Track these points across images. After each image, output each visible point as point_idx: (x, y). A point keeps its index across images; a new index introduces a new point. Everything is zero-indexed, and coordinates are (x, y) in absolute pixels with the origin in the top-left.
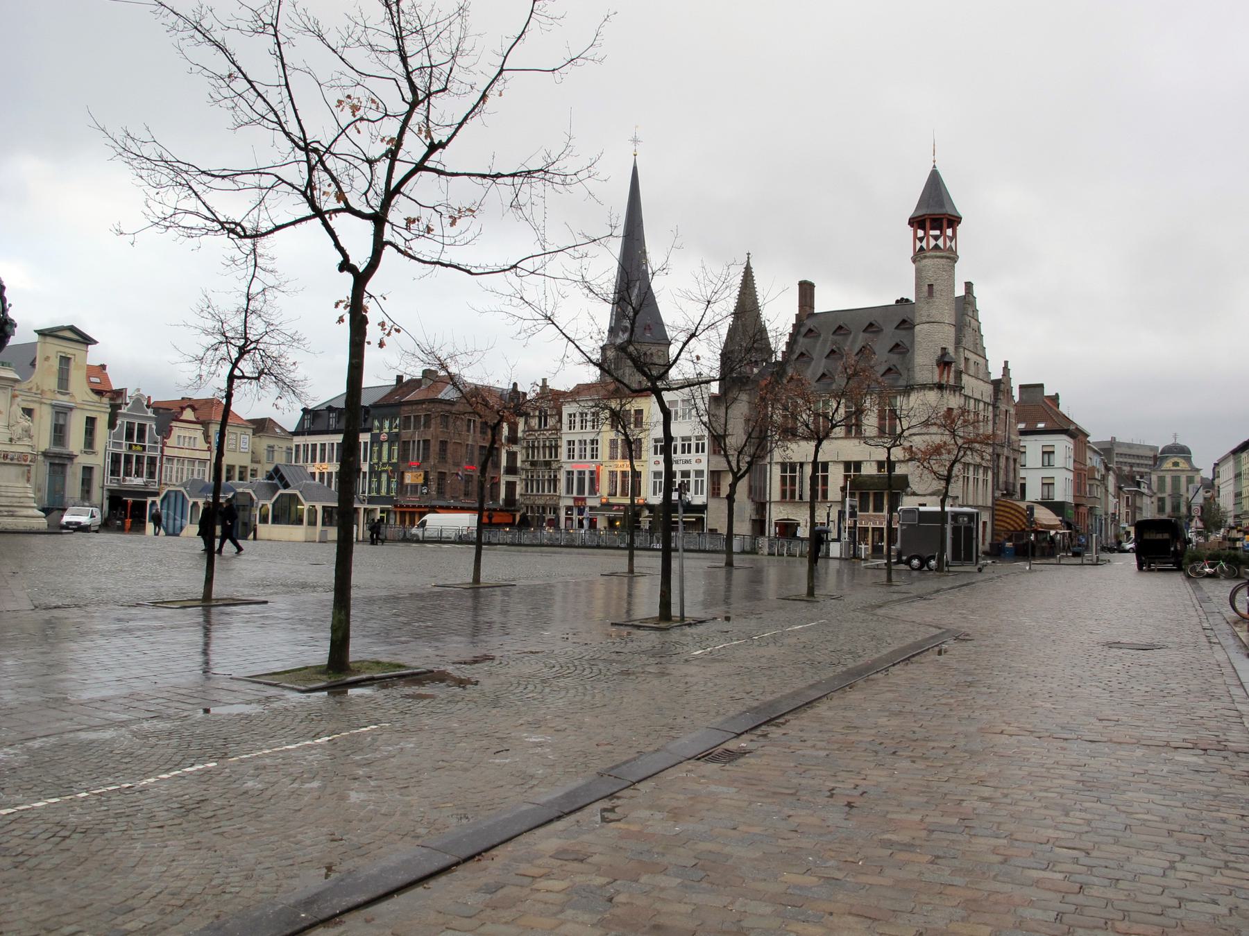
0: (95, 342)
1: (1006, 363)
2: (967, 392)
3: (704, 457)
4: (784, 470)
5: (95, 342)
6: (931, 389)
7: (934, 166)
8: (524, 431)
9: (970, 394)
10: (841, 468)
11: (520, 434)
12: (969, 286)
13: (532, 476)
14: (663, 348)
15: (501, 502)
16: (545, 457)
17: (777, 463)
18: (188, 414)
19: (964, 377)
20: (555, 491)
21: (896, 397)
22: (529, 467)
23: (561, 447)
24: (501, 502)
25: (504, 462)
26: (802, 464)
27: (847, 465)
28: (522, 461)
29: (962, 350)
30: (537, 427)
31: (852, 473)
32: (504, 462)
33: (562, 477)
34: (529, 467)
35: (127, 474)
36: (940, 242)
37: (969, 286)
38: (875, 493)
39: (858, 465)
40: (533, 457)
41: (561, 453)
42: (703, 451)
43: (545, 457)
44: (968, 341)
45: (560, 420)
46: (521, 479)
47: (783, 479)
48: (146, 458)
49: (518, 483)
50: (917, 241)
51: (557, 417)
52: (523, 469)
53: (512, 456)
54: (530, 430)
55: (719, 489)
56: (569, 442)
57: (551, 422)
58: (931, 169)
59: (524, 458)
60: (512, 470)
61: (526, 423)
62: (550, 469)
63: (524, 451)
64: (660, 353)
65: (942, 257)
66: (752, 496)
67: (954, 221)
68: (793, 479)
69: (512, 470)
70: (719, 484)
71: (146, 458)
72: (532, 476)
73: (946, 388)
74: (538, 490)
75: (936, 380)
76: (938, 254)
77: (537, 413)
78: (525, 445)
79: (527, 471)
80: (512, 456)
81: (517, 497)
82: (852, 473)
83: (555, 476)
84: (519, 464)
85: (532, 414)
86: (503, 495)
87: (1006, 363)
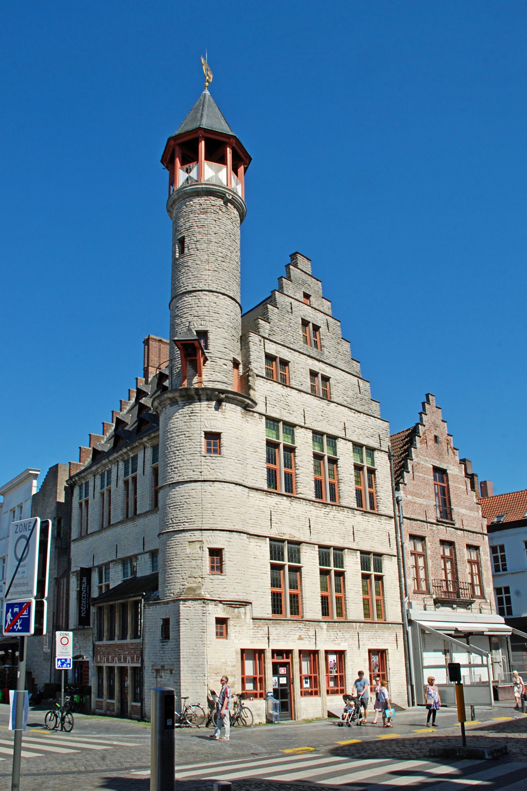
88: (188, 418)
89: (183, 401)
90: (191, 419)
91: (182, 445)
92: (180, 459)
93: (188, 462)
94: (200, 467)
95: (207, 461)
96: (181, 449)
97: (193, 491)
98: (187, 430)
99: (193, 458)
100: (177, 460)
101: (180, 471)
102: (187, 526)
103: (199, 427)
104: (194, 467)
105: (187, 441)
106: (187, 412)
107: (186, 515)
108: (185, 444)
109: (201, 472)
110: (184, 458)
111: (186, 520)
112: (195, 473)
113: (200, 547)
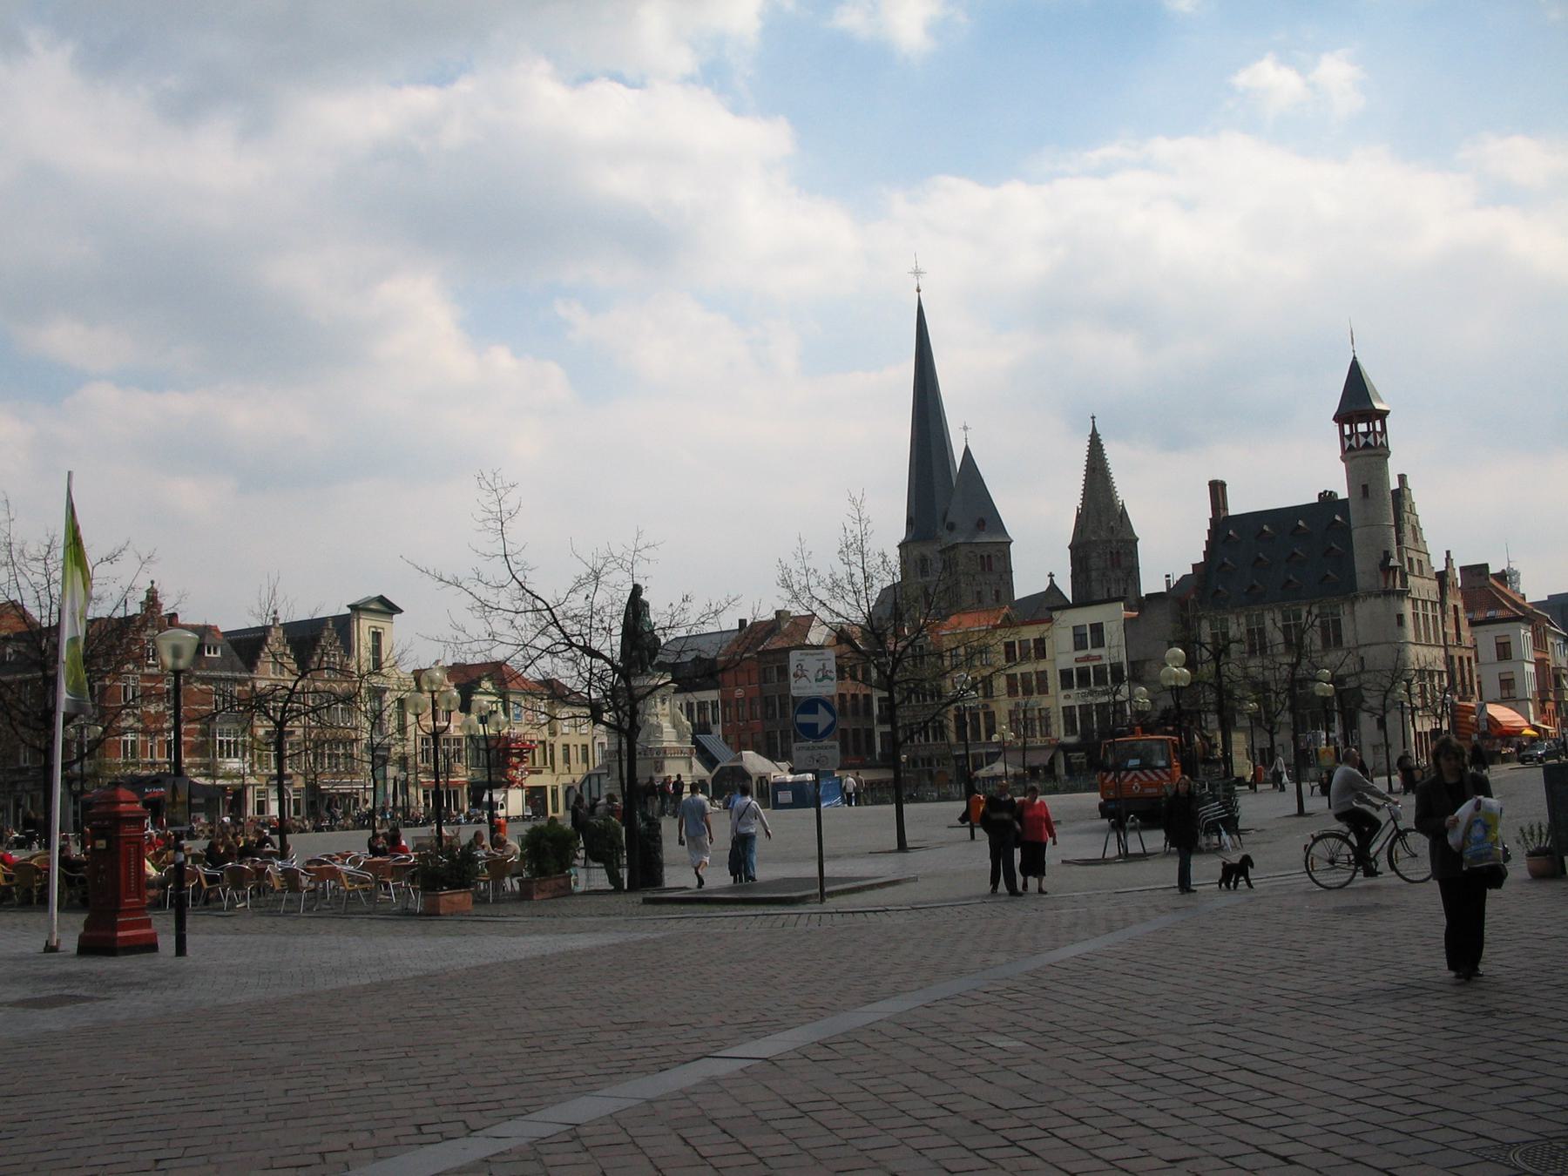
0: (401, 611)
1: (1448, 553)
2: (1415, 594)
5: (401, 611)
6: (1378, 596)
7: (1355, 358)
9: (1417, 597)
12: (1402, 478)
18: (487, 685)
19: (1410, 578)
24: (877, 757)
29: (1404, 550)
35: (856, 732)
36: (1371, 439)
37: (1402, 478)
44: (1408, 540)
48: (1077, 709)
50: (1345, 439)
71: (1077, 709)
87: (1448, 553)
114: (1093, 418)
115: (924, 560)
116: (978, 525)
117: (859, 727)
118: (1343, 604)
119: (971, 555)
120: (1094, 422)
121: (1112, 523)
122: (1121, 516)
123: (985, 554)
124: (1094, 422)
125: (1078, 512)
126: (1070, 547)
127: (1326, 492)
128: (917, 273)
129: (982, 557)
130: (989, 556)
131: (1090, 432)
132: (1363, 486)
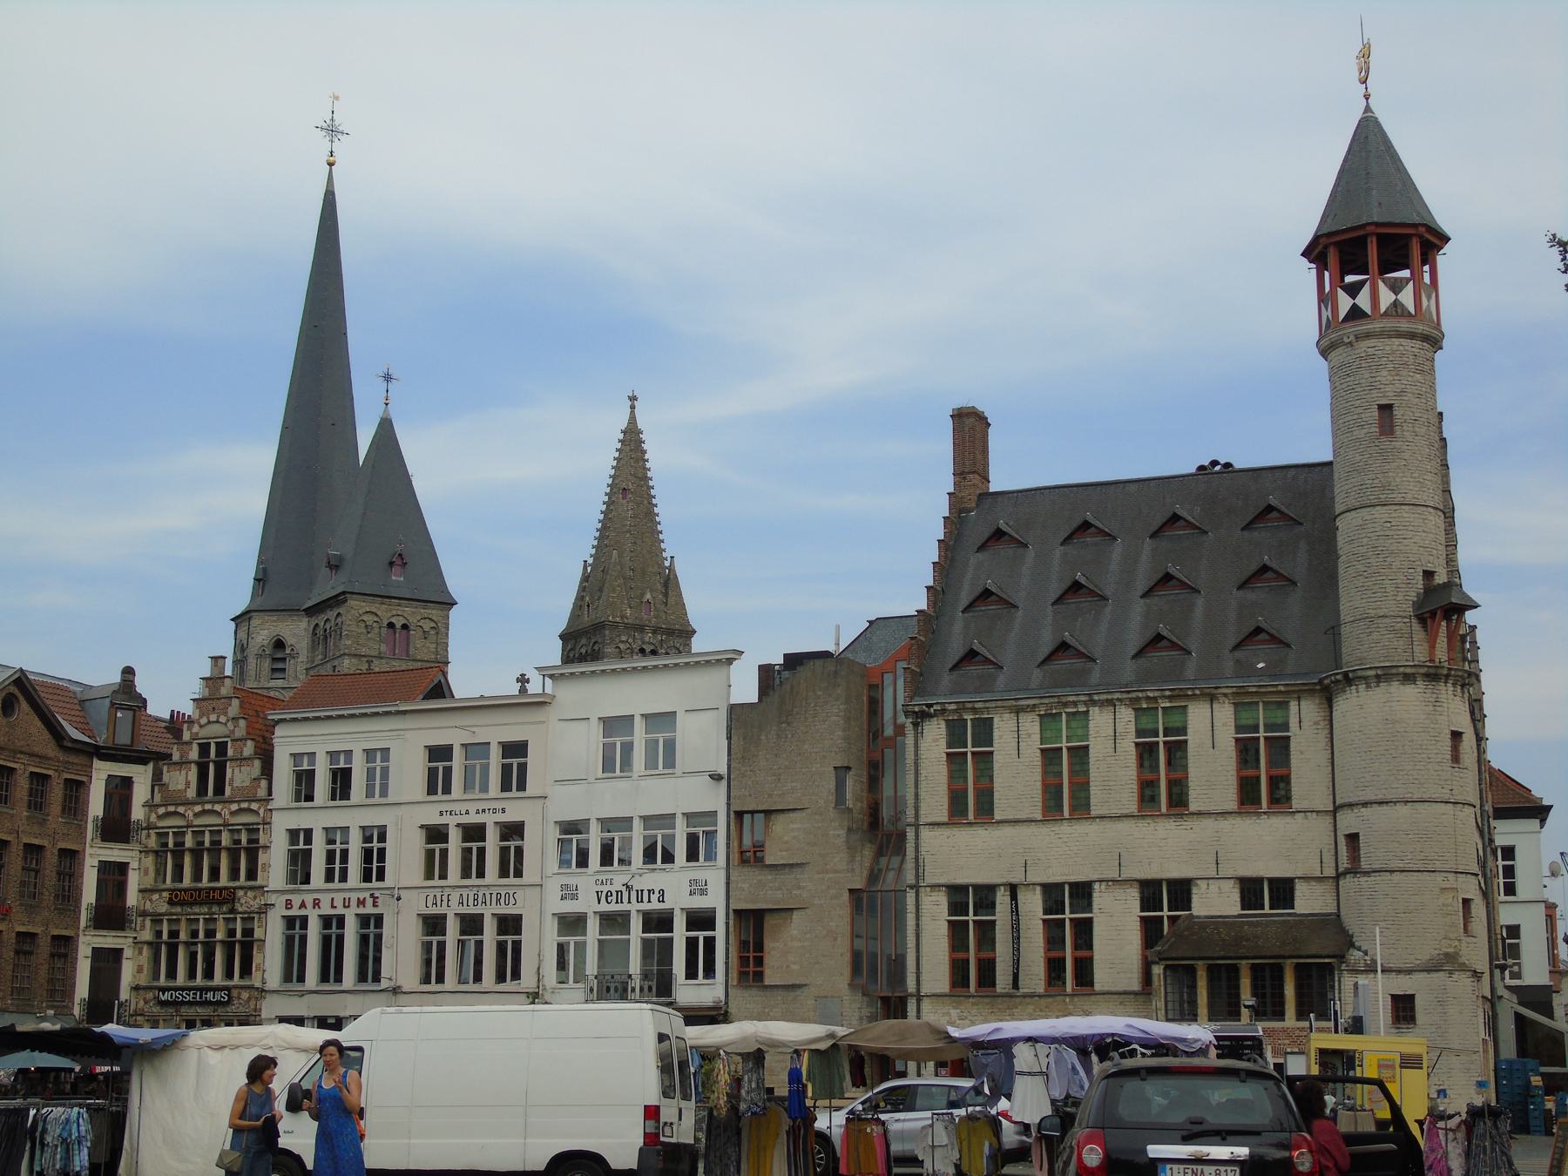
3: (714, 876)
4: (957, 907)
6: (1408, 678)
7: (1368, 109)
8: (150, 805)
10: (1133, 897)
11: (138, 813)
13: (174, 934)
14: (434, 613)
15: (77, 1011)
16: (215, 874)
17: (935, 887)
20: (246, 970)
21: (1284, 705)
22: (164, 908)
23: (266, 847)
24: (77, 1011)
25: (89, 894)
26: (1013, 889)
27: (1150, 892)
28: (141, 891)
30: (191, 793)
31: (1166, 913)
32: (89, 894)
33: (272, 935)
34: (164, 908)
38: (1254, 968)
39: (1181, 891)
40: (178, 876)
41: (266, 866)
42: (711, 856)
43: (197, 876)
45: (267, 770)
46: (136, 943)
47: (957, 932)
49: (127, 953)
51: (257, 763)
52: (144, 914)
53: (114, 875)
54: (163, 796)
55: (759, 961)
56: (293, 834)
57: (238, 776)
58: (1358, 115)
59: (149, 881)
60: (111, 914)
61: (157, 777)
62: (232, 911)
63: (149, 861)
64: (427, 625)
65: (1412, 336)
66: (863, 980)
67: (1432, 240)
68: (986, 931)
69: (111, 914)
70: (759, 947)
72: (174, 934)
73: (1447, 676)
74: (192, 974)
75: (1421, 654)
76: (1404, 325)
77: (194, 754)
78: (152, 842)
79: (157, 919)
80: (114, 875)
81: (124, 994)
82: (1166, 913)
83: (248, 932)
84: (132, 898)
85: (176, 757)
86: (82, 989)
88: (1431, 708)
89: (1424, 681)
90: (1435, 710)
91: (1424, 747)
92: (1423, 768)
93: (1436, 773)
94: (1449, 782)
95: (1456, 774)
96: (1423, 753)
97: (1444, 816)
98: (1432, 726)
99: (1441, 768)
100: (1417, 767)
101: (1425, 786)
102: (1438, 866)
103: (1447, 723)
104: (1443, 782)
105: (1433, 742)
106: (1430, 699)
107: (1437, 850)
108: (1430, 747)
109: (1451, 790)
110: (1430, 767)
111: (1436, 857)
112: (1443, 791)
113: (1453, 897)
114: (633, 399)
115: (279, 644)
116: (391, 564)
117: (38, 930)
118: (1299, 699)
119: (369, 619)
120: (633, 407)
121: (648, 596)
122: (666, 585)
123: (398, 622)
124: (633, 407)
125: (585, 568)
126: (561, 637)
127: (1214, 463)
128: (332, 131)
129: (391, 625)
130: (405, 627)
131: (624, 425)
132: (1382, 407)
